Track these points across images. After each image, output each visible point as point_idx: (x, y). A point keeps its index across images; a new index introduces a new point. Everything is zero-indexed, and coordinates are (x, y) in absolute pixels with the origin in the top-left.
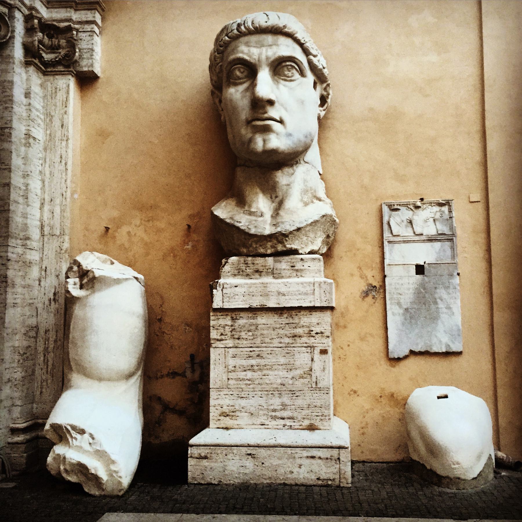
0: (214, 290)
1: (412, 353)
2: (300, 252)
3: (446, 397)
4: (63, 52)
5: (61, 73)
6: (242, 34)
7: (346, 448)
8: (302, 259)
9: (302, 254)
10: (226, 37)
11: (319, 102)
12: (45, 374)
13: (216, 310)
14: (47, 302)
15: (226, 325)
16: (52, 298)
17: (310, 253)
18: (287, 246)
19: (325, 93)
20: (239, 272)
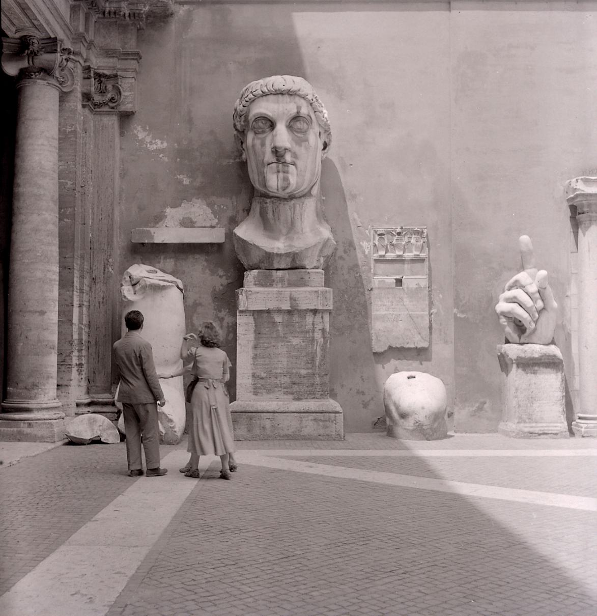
0: (240, 296)
1: (390, 348)
2: (307, 267)
3: (414, 377)
4: (109, 96)
5: (108, 113)
6: (265, 94)
7: (341, 413)
8: (309, 273)
9: (308, 269)
10: (251, 94)
11: (322, 148)
12: (97, 362)
13: (241, 312)
14: (97, 305)
15: (249, 323)
16: (101, 301)
17: (314, 269)
18: (298, 262)
19: (327, 141)
20: (259, 283)
